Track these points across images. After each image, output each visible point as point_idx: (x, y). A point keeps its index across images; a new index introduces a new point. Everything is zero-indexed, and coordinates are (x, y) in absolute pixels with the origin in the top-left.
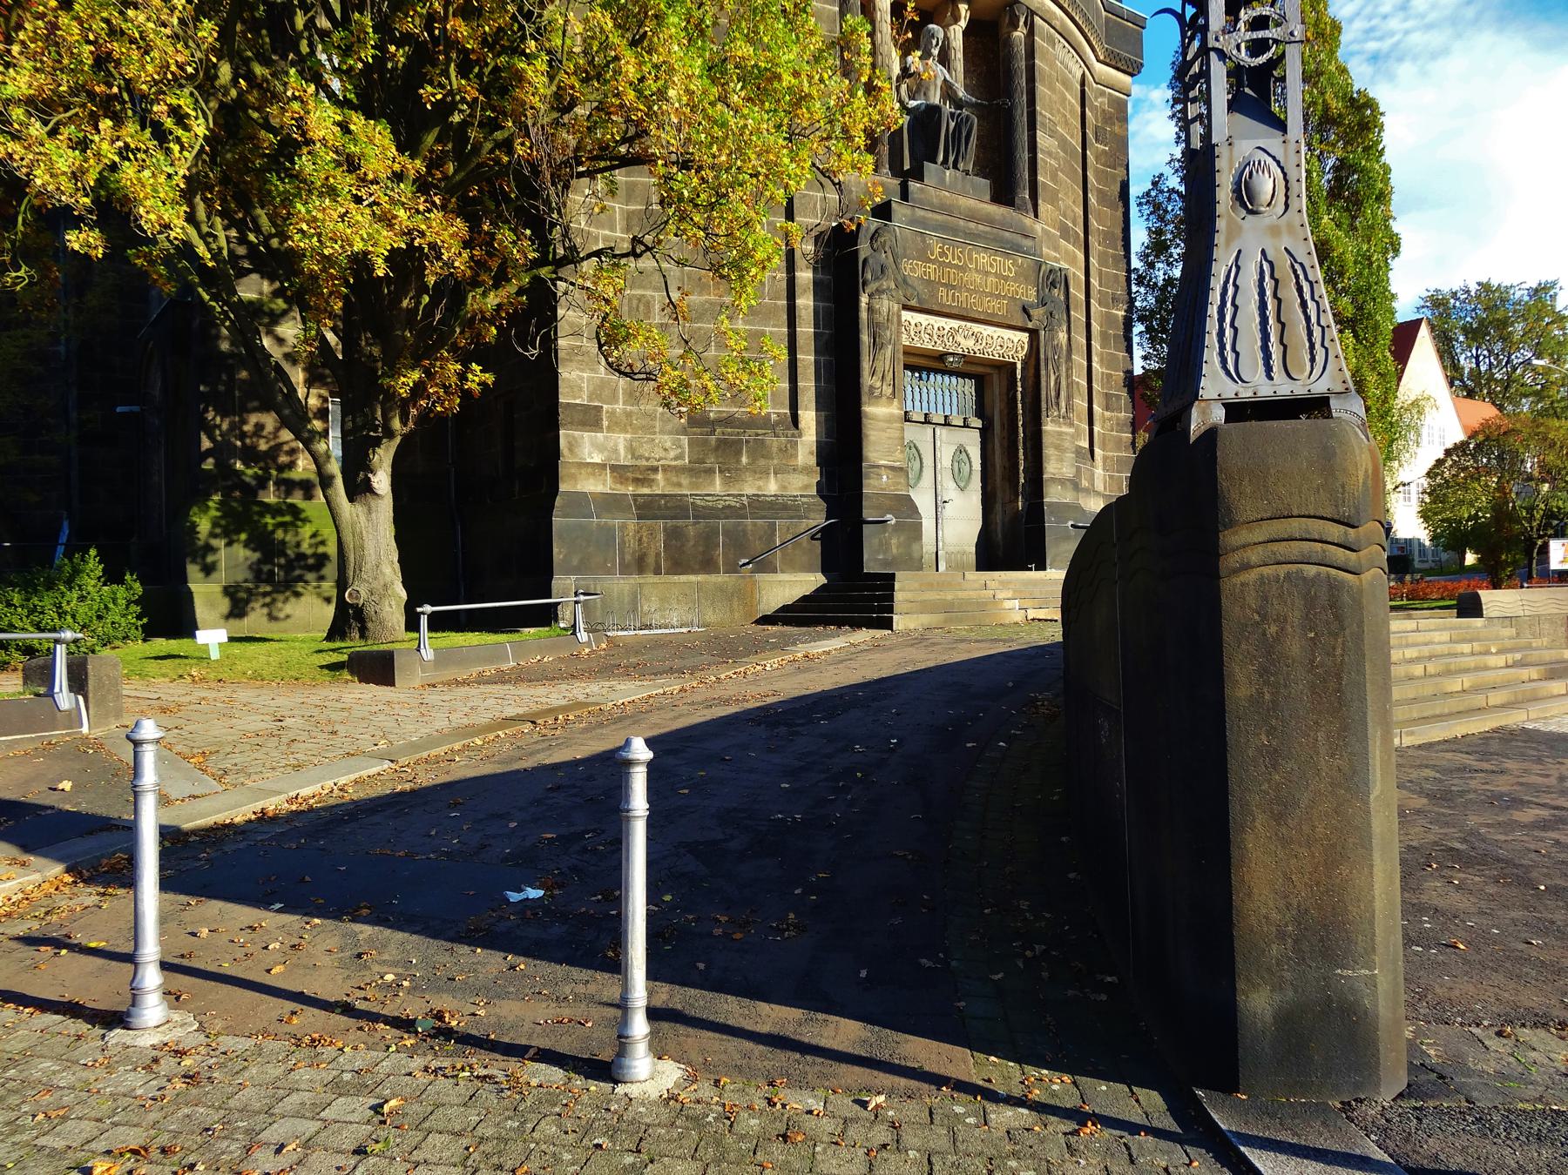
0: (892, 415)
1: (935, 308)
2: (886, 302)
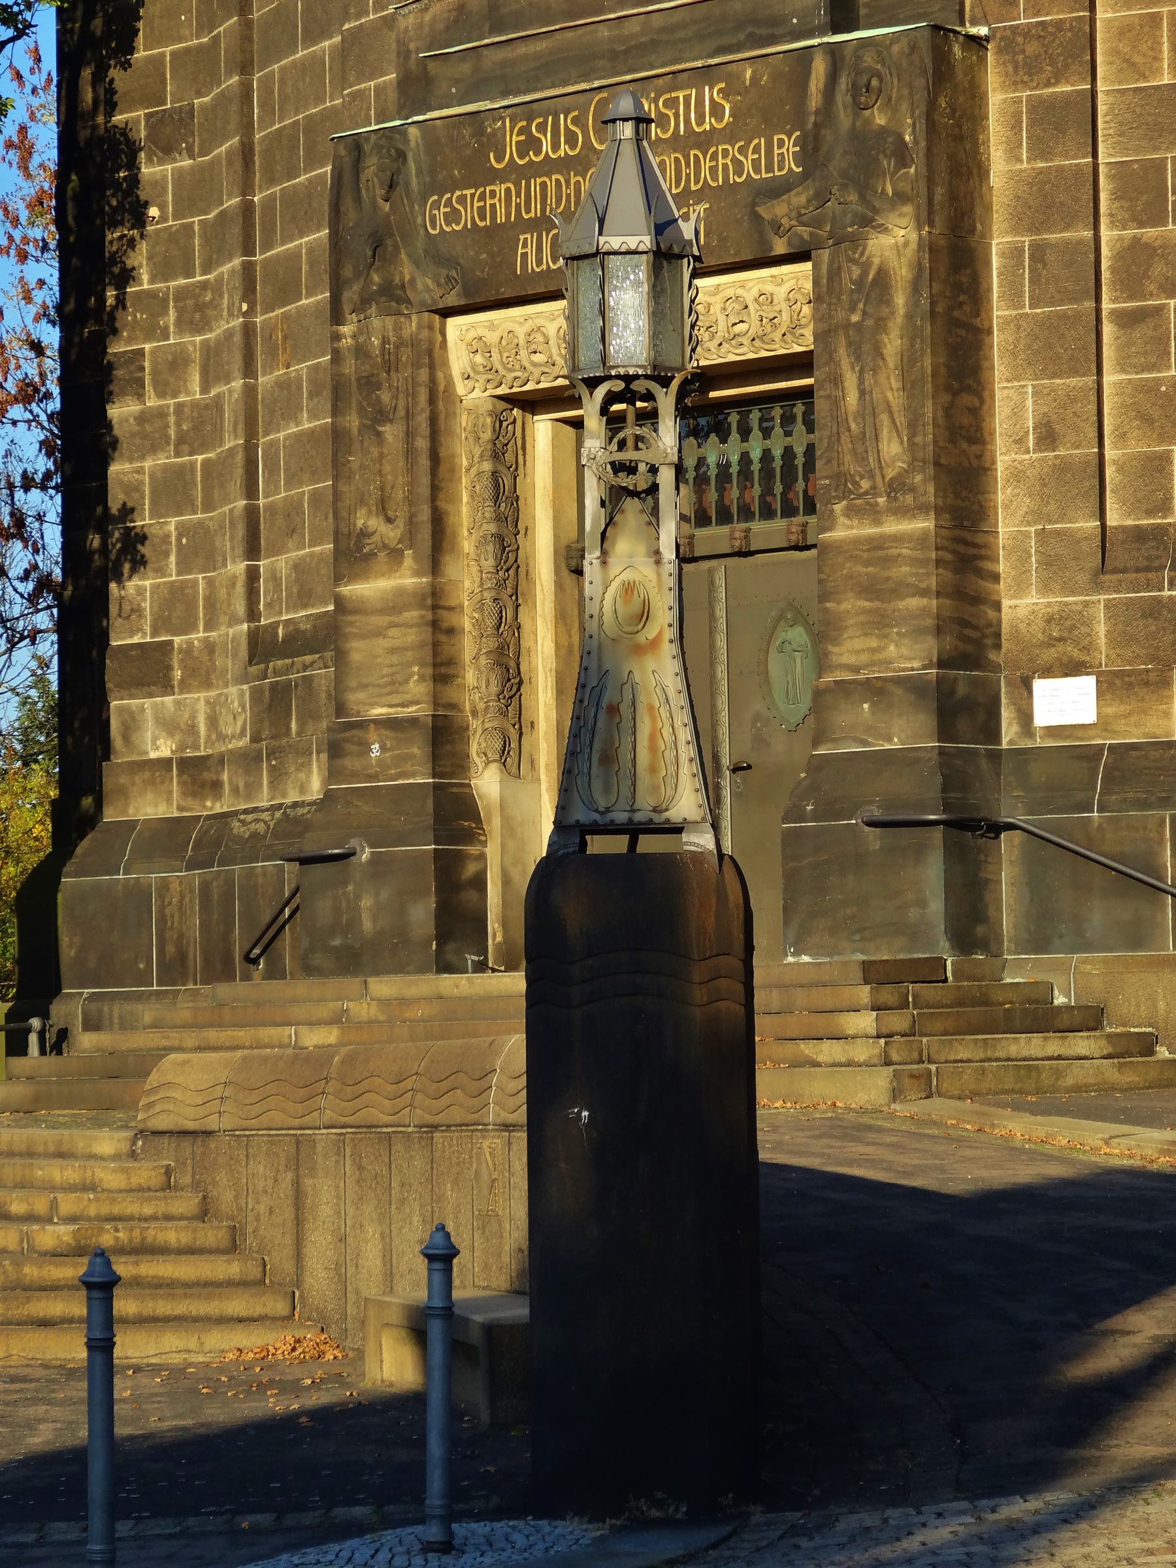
0: (400, 592)
1: (507, 292)
2: (376, 322)
